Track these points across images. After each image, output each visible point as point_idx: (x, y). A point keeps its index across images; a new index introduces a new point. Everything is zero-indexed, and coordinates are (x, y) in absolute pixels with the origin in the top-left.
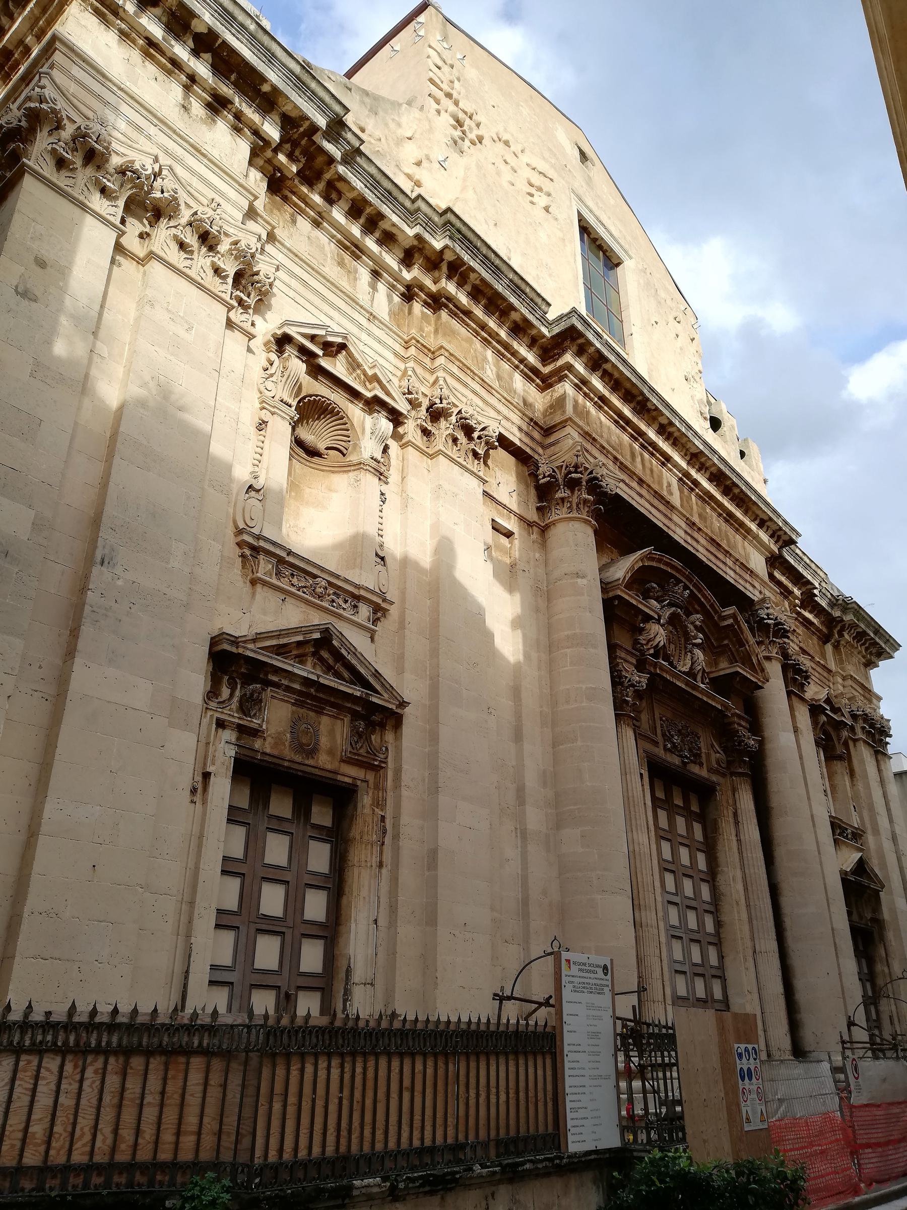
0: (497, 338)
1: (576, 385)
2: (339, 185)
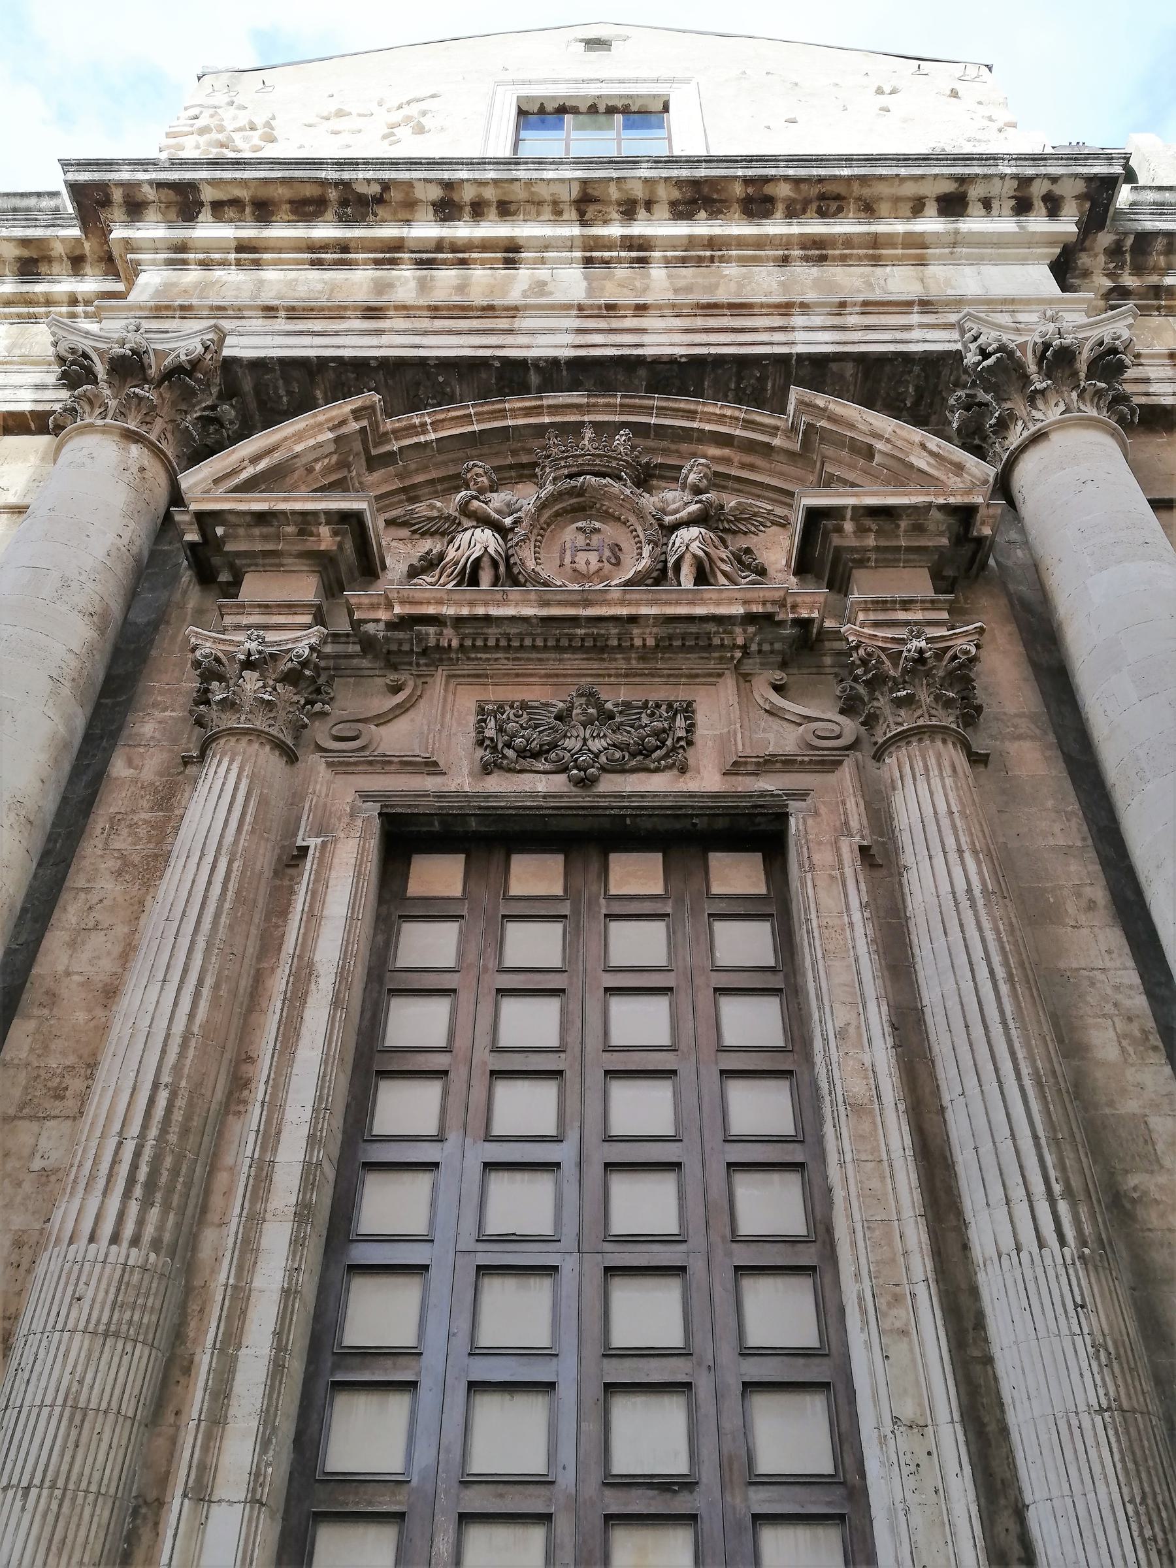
1: (170, 262)
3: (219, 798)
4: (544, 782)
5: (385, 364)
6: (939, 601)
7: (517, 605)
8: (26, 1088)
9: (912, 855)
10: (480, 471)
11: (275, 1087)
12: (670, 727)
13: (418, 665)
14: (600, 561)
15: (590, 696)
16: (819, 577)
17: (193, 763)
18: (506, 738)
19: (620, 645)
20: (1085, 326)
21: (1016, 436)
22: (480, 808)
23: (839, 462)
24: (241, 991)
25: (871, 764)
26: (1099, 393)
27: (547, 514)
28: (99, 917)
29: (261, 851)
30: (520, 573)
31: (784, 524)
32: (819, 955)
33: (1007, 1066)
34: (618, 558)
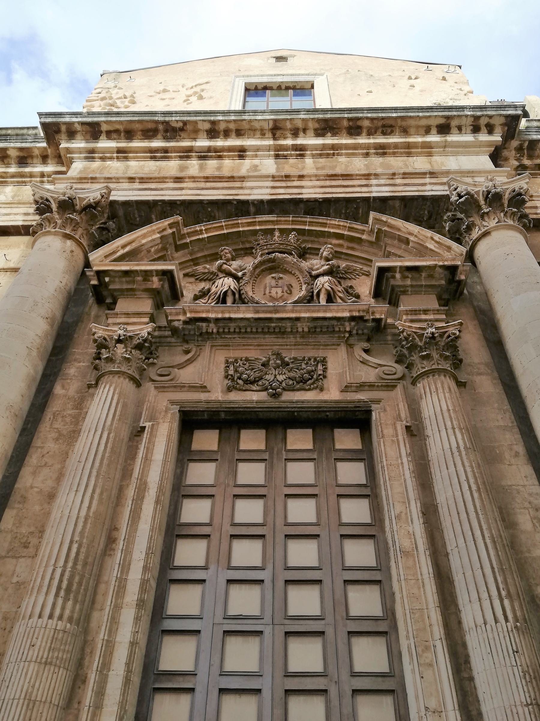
0: (8, 175)
1: (86, 158)
3: (104, 404)
4: (256, 396)
5: (183, 202)
6: (441, 310)
7: (244, 313)
8: (11, 543)
9: (430, 430)
10: (227, 251)
11: (128, 542)
12: (315, 370)
13: (198, 340)
14: (283, 292)
15: (278, 355)
16: (384, 299)
17: (93, 387)
18: (239, 375)
19: (292, 331)
20: (507, 183)
21: (475, 233)
22: (226, 408)
23: (394, 246)
24: (113, 496)
25: (410, 386)
26: (514, 214)
27: (258, 271)
28: (46, 460)
29: (123, 429)
30: (245, 298)
31: (368, 275)
32: (387, 479)
33: (478, 533)
34: (291, 291)
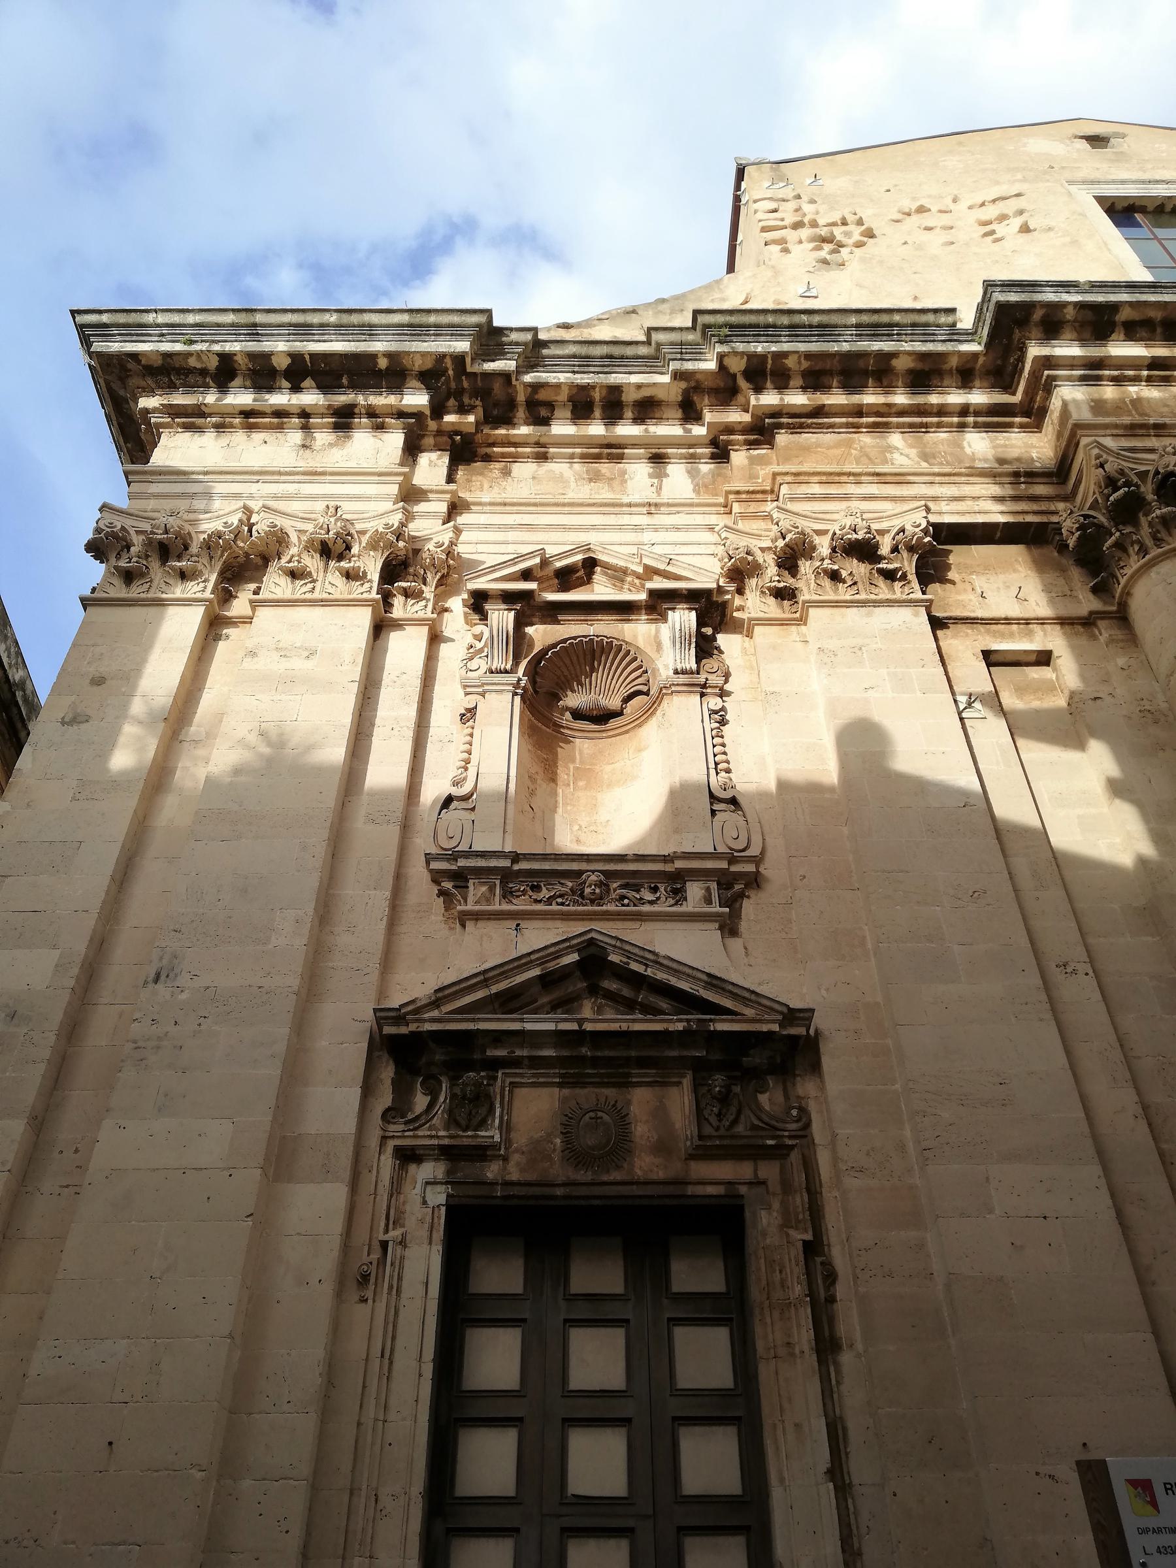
0: (894, 410)
1: (1083, 379)
2: (542, 395)
